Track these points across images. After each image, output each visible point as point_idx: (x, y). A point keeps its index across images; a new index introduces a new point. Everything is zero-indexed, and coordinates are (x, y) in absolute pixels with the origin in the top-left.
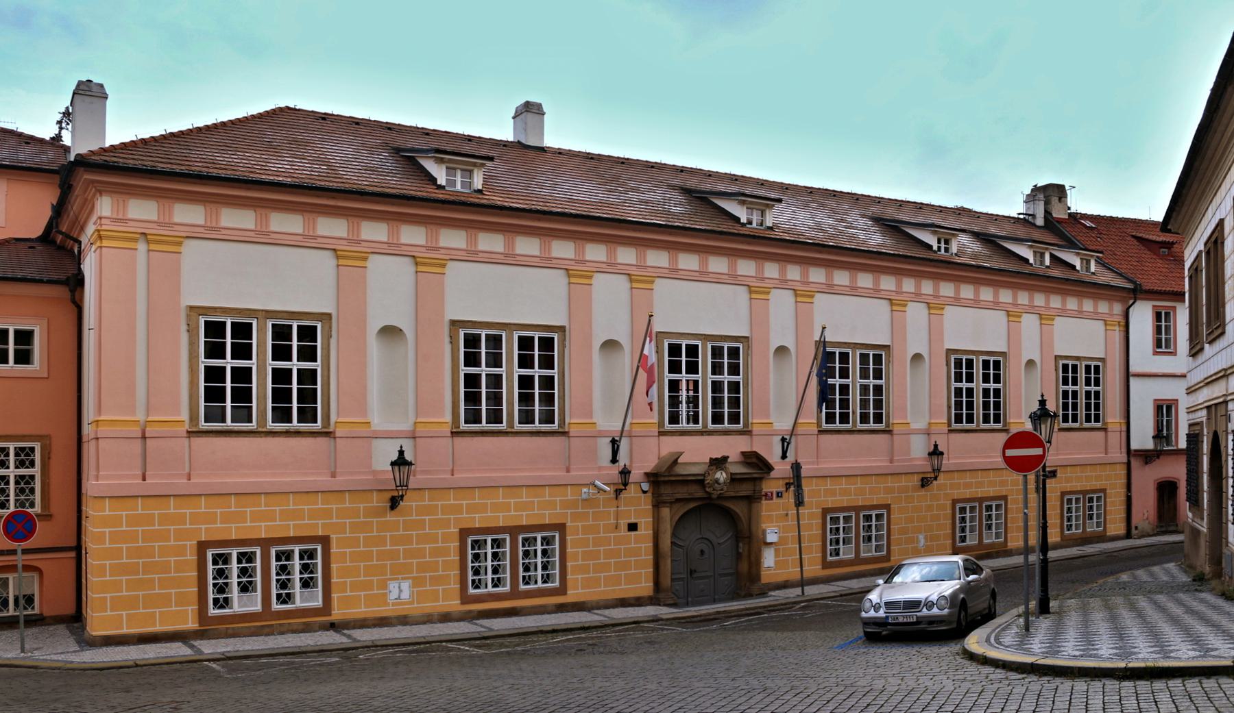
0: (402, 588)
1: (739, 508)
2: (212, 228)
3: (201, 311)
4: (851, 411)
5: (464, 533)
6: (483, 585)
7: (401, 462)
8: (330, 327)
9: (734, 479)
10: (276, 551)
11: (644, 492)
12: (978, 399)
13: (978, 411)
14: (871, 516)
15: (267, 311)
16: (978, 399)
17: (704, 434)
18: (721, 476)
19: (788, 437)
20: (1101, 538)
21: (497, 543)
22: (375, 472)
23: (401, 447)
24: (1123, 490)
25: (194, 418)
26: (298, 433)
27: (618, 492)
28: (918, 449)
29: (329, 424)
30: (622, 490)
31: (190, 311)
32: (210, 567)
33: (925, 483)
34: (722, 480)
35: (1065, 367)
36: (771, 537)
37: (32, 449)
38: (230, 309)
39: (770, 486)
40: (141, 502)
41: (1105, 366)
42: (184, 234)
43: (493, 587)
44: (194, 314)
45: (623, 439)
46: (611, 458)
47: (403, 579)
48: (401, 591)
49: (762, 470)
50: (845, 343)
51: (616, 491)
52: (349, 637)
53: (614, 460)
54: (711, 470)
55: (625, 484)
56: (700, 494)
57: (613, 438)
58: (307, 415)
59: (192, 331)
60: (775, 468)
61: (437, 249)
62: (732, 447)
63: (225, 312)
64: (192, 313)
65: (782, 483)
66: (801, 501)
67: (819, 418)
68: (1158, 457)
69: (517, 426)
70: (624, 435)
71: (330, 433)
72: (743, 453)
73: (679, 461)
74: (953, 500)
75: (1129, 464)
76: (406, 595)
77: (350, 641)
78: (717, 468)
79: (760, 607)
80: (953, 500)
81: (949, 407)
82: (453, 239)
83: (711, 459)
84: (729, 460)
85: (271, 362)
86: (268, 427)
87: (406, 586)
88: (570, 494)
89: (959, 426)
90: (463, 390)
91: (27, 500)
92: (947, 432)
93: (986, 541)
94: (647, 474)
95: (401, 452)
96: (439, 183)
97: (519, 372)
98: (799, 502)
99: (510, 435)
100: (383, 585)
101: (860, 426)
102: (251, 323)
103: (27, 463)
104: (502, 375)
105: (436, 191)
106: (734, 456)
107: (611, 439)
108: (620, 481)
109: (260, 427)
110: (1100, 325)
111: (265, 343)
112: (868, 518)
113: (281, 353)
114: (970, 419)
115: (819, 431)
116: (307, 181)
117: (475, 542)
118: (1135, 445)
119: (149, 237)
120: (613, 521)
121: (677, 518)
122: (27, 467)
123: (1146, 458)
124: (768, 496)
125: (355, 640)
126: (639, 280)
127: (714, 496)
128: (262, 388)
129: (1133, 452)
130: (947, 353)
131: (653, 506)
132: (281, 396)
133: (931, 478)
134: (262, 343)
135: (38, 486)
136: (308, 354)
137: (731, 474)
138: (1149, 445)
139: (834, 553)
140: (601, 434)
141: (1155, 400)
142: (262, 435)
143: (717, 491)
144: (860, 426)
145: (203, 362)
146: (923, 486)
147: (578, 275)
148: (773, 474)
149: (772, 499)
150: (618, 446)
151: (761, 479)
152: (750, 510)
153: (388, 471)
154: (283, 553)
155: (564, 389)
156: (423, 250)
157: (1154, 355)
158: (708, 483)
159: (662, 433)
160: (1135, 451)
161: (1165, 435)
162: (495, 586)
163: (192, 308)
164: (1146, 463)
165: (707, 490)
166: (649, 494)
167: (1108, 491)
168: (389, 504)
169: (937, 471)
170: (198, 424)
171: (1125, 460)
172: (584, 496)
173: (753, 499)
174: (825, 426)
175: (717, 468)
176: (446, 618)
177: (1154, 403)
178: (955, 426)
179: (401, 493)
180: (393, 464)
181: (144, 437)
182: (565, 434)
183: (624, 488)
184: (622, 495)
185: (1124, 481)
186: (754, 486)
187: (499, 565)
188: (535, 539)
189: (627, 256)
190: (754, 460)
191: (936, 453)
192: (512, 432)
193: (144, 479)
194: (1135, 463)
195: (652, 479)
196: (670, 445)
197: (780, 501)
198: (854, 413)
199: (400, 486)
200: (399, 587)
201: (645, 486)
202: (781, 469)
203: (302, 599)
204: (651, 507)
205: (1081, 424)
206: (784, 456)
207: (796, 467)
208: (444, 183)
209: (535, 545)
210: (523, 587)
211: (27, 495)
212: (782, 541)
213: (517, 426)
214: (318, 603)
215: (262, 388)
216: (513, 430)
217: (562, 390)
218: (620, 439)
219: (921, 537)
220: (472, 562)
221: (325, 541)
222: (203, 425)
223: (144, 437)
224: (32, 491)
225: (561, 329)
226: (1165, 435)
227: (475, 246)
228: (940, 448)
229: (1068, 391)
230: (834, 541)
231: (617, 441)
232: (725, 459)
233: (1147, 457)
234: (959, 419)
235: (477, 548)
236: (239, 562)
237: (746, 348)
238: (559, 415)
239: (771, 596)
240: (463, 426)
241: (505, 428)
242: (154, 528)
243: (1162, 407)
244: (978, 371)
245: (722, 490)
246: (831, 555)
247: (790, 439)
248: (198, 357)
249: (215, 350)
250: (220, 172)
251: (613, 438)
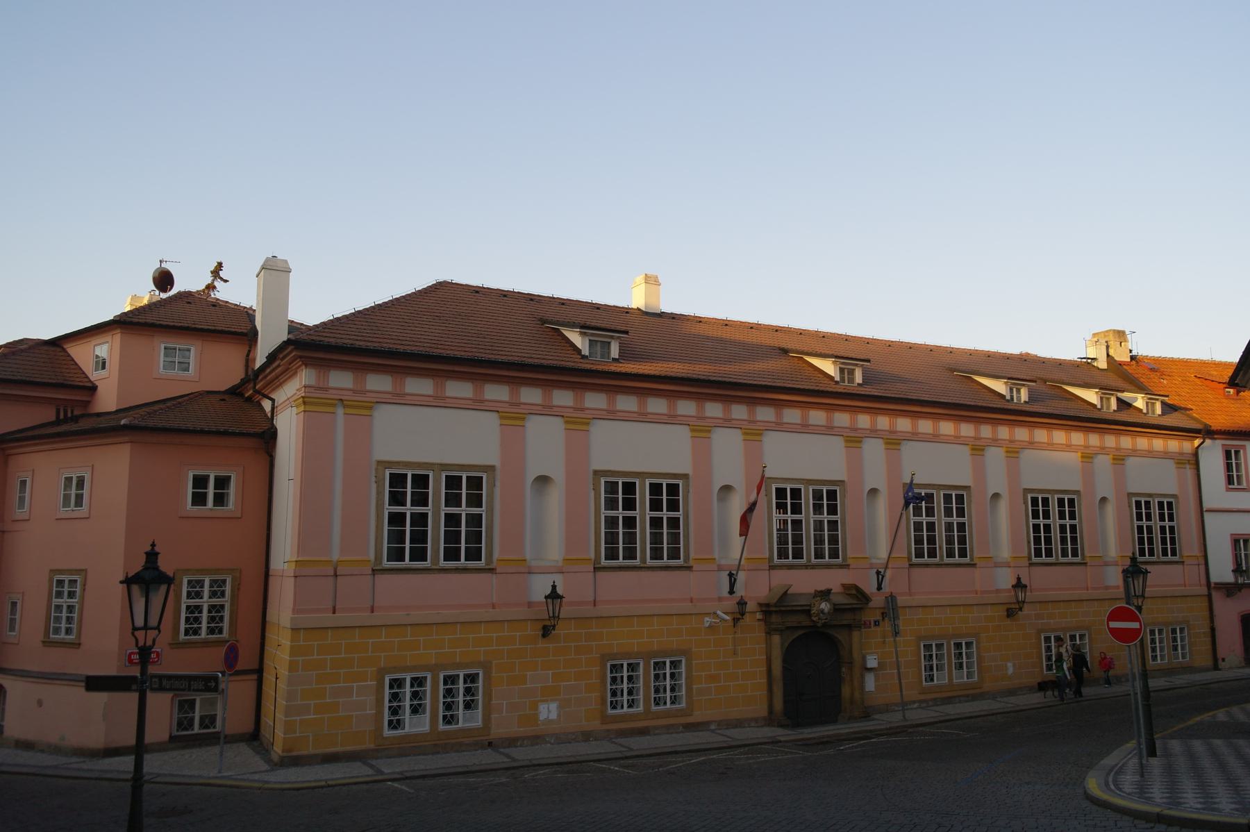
0: (550, 708)
1: (841, 636)
2: (398, 395)
6: (619, 707)
7: (554, 595)
9: (837, 609)
10: (444, 676)
12: (1056, 535)
13: (1056, 545)
14: (961, 644)
15: (441, 465)
16: (1056, 535)
17: (809, 567)
18: (825, 606)
19: (882, 570)
20: (1190, 669)
21: (632, 667)
23: (554, 582)
26: (465, 570)
27: (735, 621)
28: (1005, 580)
29: (492, 562)
30: (739, 619)
32: (387, 691)
33: (1010, 613)
34: (826, 610)
35: (1138, 504)
36: (872, 662)
37: (224, 581)
39: (870, 616)
41: (1177, 503)
42: (375, 400)
43: (629, 707)
45: (740, 572)
46: (728, 590)
47: (552, 700)
48: (549, 711)
50: (930, 485)
51: (734, 619)
52: (508, 756)
53: (731, 592)
55: (743, 614)
56: (807, 623)
57: (730, 572)
58: (474, 554)
59: (379, 482)
60: (873, 599)
61: (583, 410)
62: (833, 580)
65: (878, 612)
66: (897, 631)
67: (909, 553)
68: (1240, 590)
69: (649, 562)
70: (741, 568)
71: (493, 569)
72: (843, 585)
73: (789, 592)
75: (1209, 597)
76: (553, 716)
77: (508, 760)
78: (821, 600)
79: (871, 731)
81: (1029, 542)
82: (595, 401)
83: (816, 591)
84: (832, 591)
87: (554, 706)
89: (1038, 560)
91: (217, 627)
92: (1028, 565)
94: (760, 605)
95: (554, 587)
96: (583, 353)
98: (896, 633)
99: (643, 570)
100: (535, 706)
101: (947, 560)
102: (429, 475)
103: (219, 593)
104: (636, 517)
105: (582, 361)
106: (836, 588)
107: (728, 572)
108: (738, 611)
112: (958, 646)
113: (453, 500)
114: (1049, 553)
115: (910, 565)
116: (477, 355)
117: (613, 666)
118: (1214, 578)
119: (345, 402)
121: (786, 645)
122: (219, 598)
124: (867, 625)
125: (514, 760)
126: (753, 433)
127: (819, 625)
128: (436, 532)
129: (1213, 585)
130: (1024, 492)
131: (766, 633)
132: (453, 537)
134: (437, 492)
135: (226, 614)
136: (475, 500)
137: (834, 605)
138: (1229, 578)
139: (928, 679)
140: (720, 568)
141: (1232, 535)
144: (947, 560)
147: (701, 430)
148: (871, 604)
149: (870, 627)
150: (735, 580)
151: (861, 609)
154: (450, 677)
155: (688, 529)
156: (571, 410)
157: (1227, 491)
159: (772, 567)
160: (1216, 584)
161: (1244, 568)
162: (630, 706)
163: (379, 462)
164: (1228, 596)
167: (1191, 623)
168: (541, 633)
169: (1021, 604)
170: (381, 563)
172: (707, 625)
175: (821, 600)
176: (587, 736)
177: (1231, 537)
178: (1035, 560)
179: (553, 623)
180: (546, 597)
181: (336, 575)
182: (689, 568)
183: (739, 616)
184: (741, 623)
185: (1206, 613)
187: (633, 687)
188: (664, 663)
189: (739, 412)
190: (854, 592)
191: (1019, 585)
192: (644, 567)
193: (334, 613)
194: (1216, 595)
195: (764, 609)
196: (782, 579)
197: (878, 629)
198: (941, 548)
200: (548, 708)
201: (759, 616)
202: (878, 601)
203: (468, 721)
204: (764, 634)
205: (1158, 557)
207: (892, 598)
208: (587, 354)
209: (664, 668)
210: (654, 708)
211: (217, 623)
212: (881, 665)
213: (649, 562)
214: (478, 722)
215: (436, 532)
216: (645, 565)
218: (737, 573)
219: (1010, 665)
220: (611, 685)
221: (486, 666)
222: (386, 564)
223: (336, 575)
224: (222, 618)
225: (685, 477)
226: (1244, 568)
228: (1024, 581)
229: (1143, 526)
231: (734, 574)
232: (829, 591)
234: (1038, 553)
235: (614, 671)
236: (412, 686)
238: (684, 552)
240: (604, 562)
243: (1239, 541)
244: (1054, 508)
245: (826, 619)
247: (885, 572)
248: (383, 504)
249: (397, 499)
250: (406, 347)
251: (730, 572)
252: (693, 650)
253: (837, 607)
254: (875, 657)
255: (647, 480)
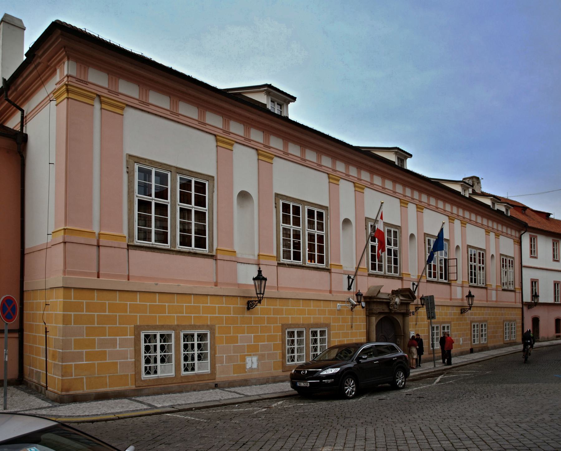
1: (399, 319)
3: (136, 160)
4: (436, 271)
5: (284, 327)
8: (214, 186)
17: (385, 277)
22: (239, 285)
24: (521, 321)
25: (131, 235)
26: (195, 254)
31: (129, 159)
38: (154, 161)
40: (158, 296)
44: (131, 161)
49: (411, 299)
54: (394, 297)
56: (387, 310)
59: (130, 173)
62: (397, 285)
63: (152, 163)
64: (130, 160)
74: (471, 321)
75: (522, 308)
80: (471, 321)
85: (179, 203)
86: (177, 248)
88: (332, 306)
90: (307, 242)
93: (481, 342)
97: (309, 231)
109: (172, 247)
110: (512, 241)
111: (176, 189)
118: (525, 300)
123: (529, 306)
129: (524, 303)
131: (366, 315)
133: (467, 309)
141: (531, 279)
142: (174, 253)
145: (137, 196)
146: (461, 313)
152: (404, 321)
153: (251, 285)
158: (392, 304)
160: (526, 302)
163: (130, 156)
164: (529, 308)
165: (391, 308)
166: (365, 309)
170: (133, 241)
171: (521, 307)
172: (338, 308)
173: (406, 314)
174: (371, 271)
185: (521, 316)
186: (407, 307)
190: (408, 293)
198: (438, 273)
199: (260, 294)
204: (365, 316)
206: (349, 288)
217: (327, 245)
221: (212, 328)
227: (268, 142)
233: (530, 306)
237: (400, 232)
241: (302, 264)
242: (183, 315)
248: (133, 191)
252: (331, 324)
255: (306, 206)
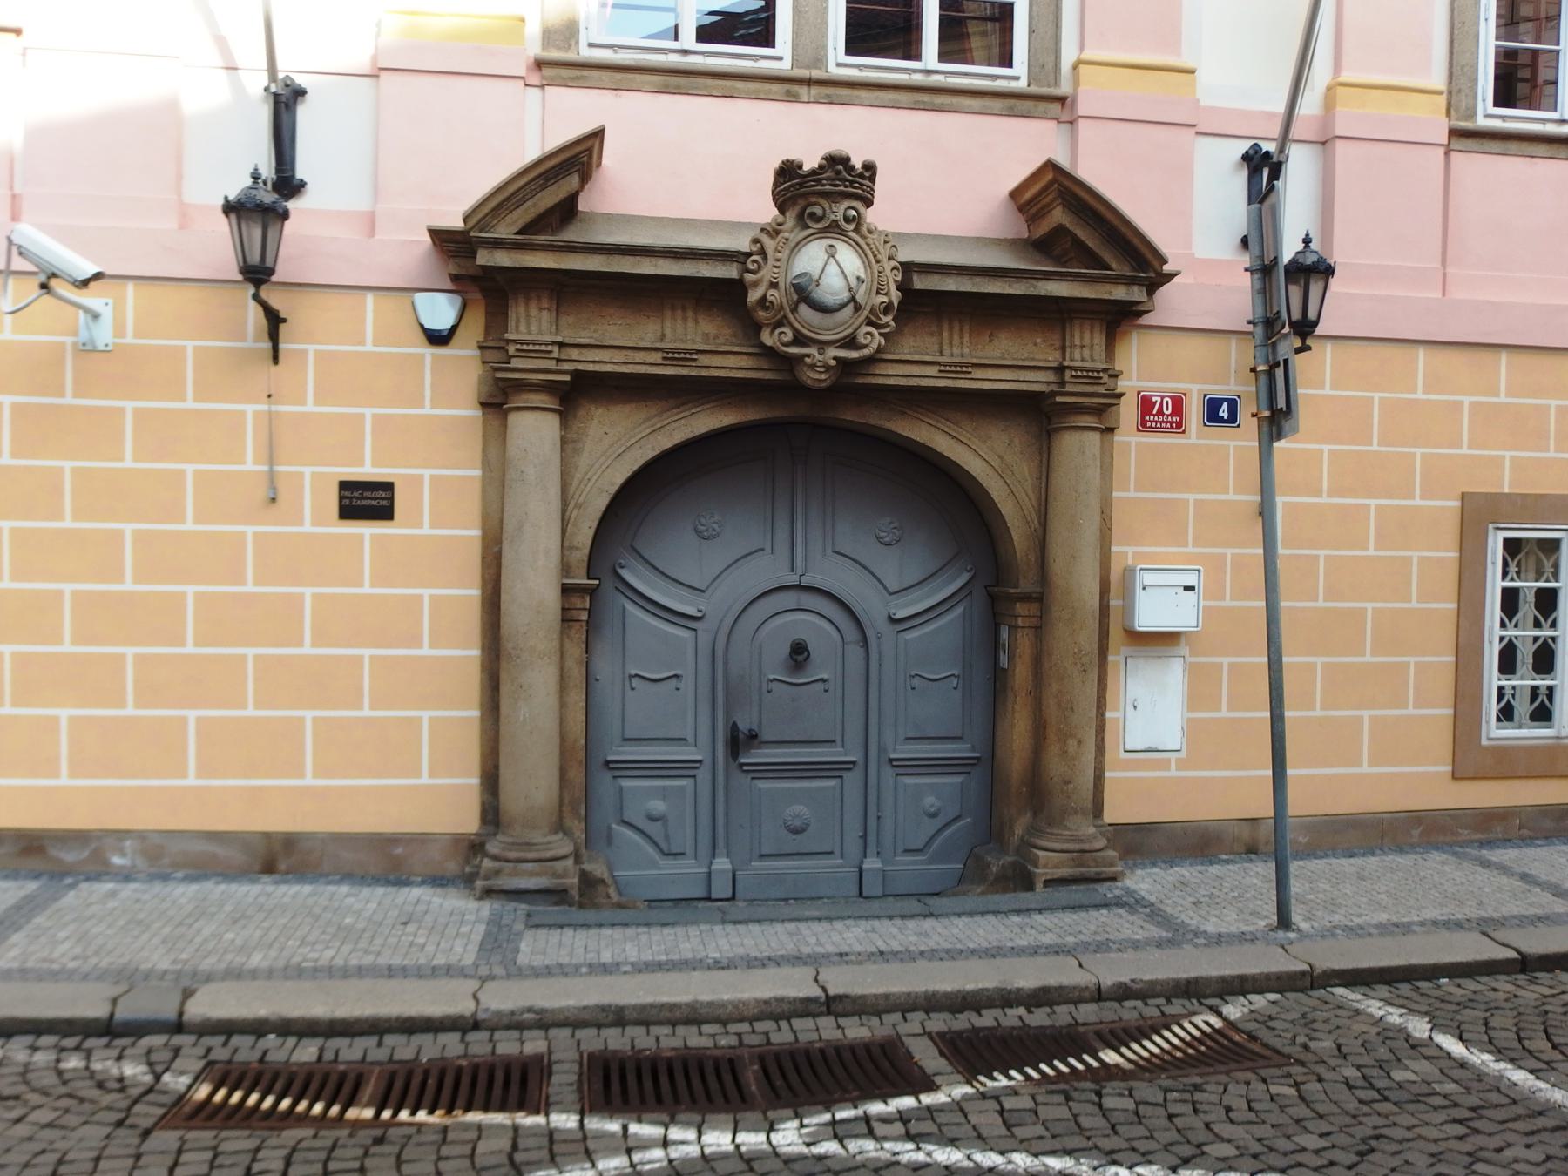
11: (437, 339)
56: (735, 365)
120: (251, 464)
131: (484, 405)
143: (822, 345)
165: (767, 338)
166: (465, 354)
204: (479, 413)
230: (1526, 654)
239: (1132, 903)
245: (851, 342)
246: (1506, 714)
253: (920, 283)
254: (1191, 580)
